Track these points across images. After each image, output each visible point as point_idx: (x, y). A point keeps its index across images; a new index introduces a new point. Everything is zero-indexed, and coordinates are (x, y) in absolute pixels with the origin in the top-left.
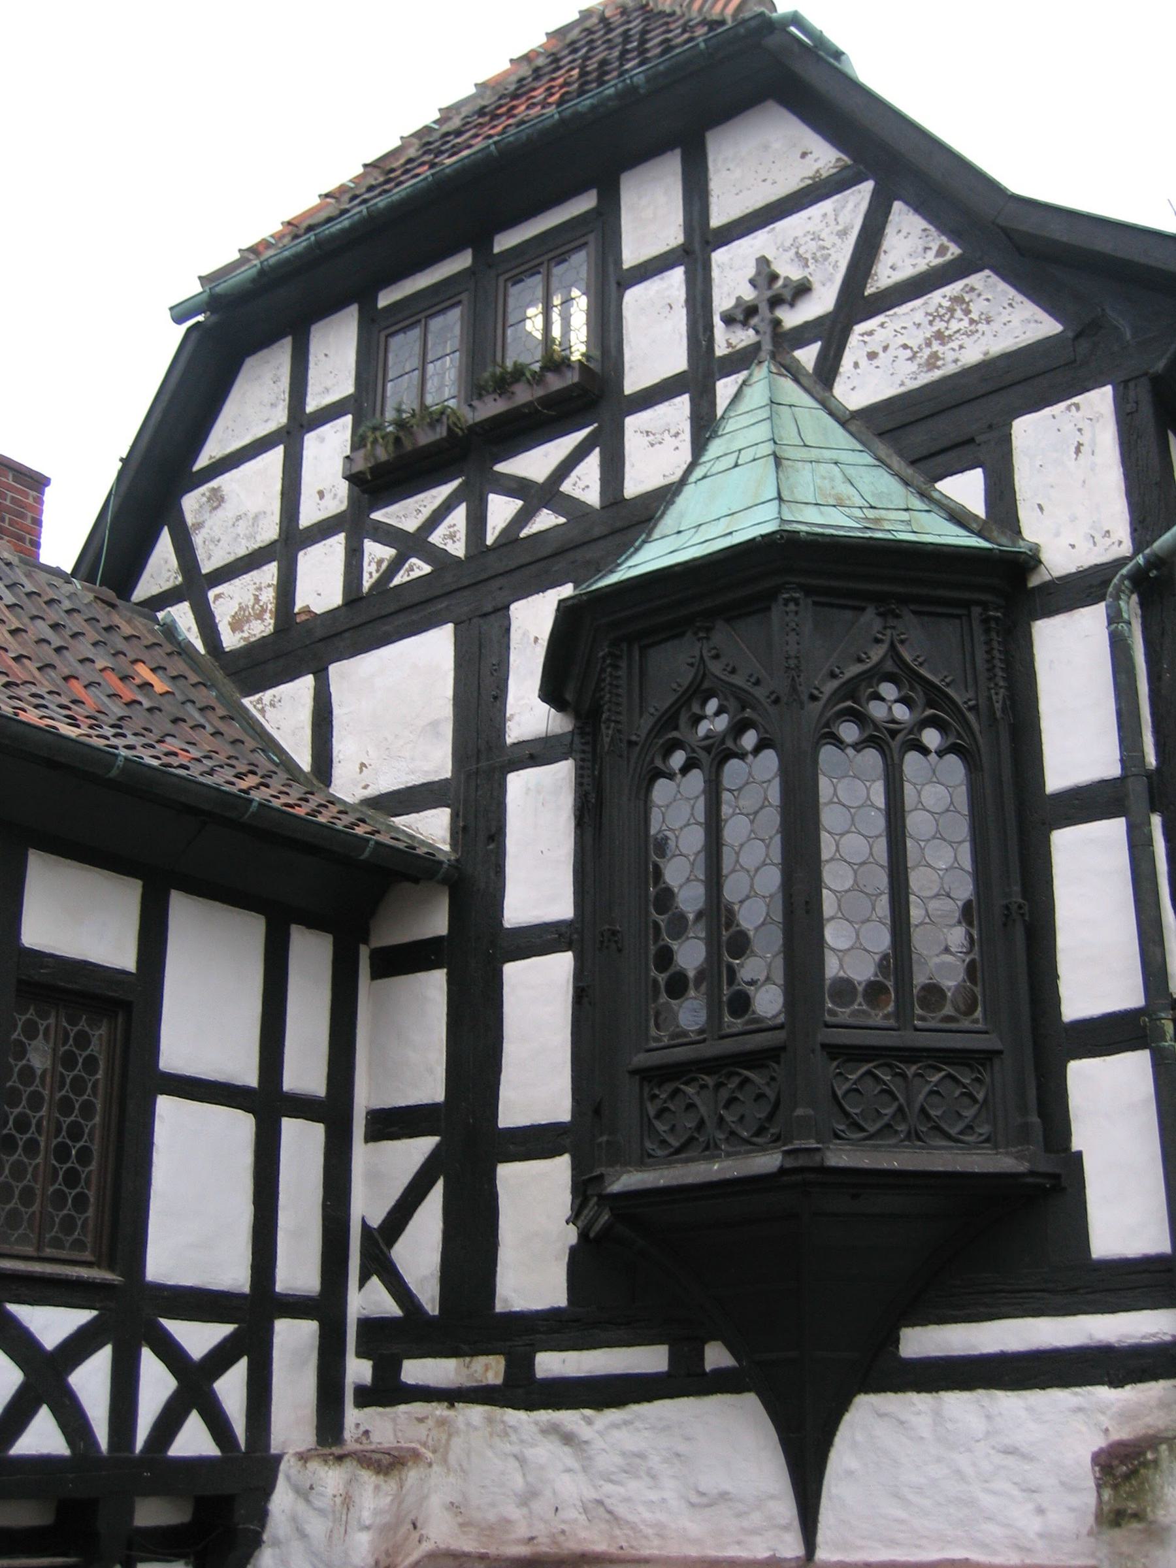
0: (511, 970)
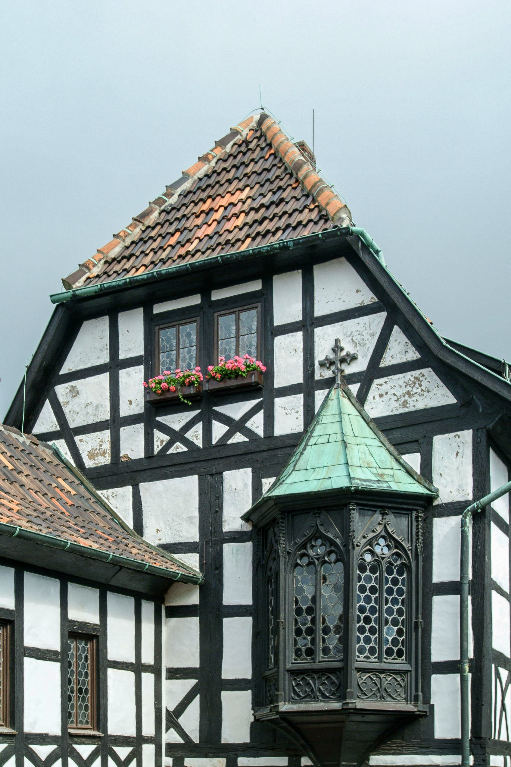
0: (226, 621)
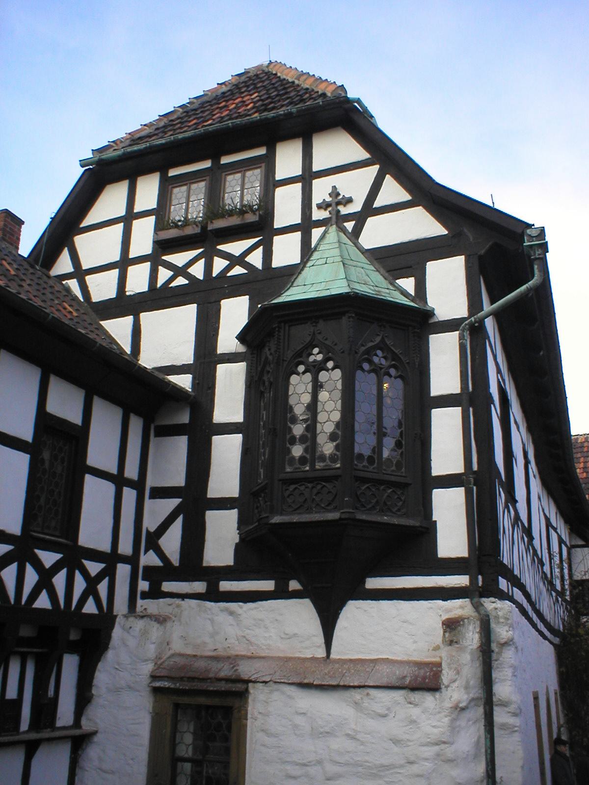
0: (216, 439)
